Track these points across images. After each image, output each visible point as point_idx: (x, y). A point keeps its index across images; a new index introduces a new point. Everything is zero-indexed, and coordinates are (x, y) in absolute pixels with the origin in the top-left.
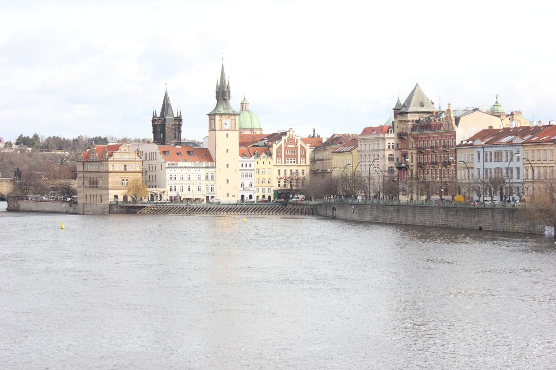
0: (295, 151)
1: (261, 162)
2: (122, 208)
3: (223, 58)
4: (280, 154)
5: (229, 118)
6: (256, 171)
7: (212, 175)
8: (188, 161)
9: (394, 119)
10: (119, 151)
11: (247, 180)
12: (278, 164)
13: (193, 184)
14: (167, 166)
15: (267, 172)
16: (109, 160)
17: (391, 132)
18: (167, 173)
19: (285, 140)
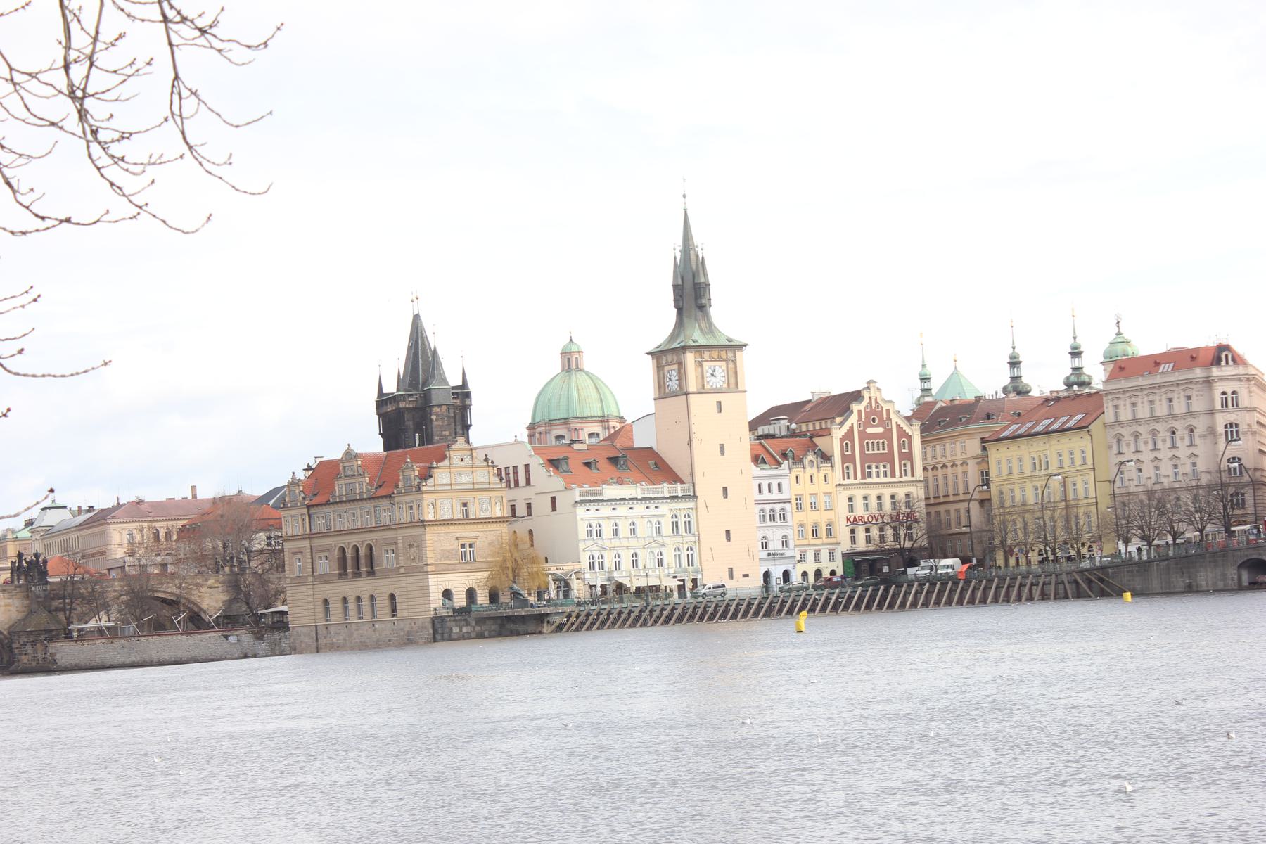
0: (886, 443)
1: (805, 478)
2: (485, 623)
3: (686, 193)
4: (849, 453)
5: (720, 359)
6: (794, 502)
7: (687, 519)
10: (446, 463)
11: (774, 529)
12: (847, 482)
13: (644, 547)
14: (578, 499)
15: (821, 505)
16: (424, 488)
17: (1227, 363)
18: (579, 518)
19: (860, 412)
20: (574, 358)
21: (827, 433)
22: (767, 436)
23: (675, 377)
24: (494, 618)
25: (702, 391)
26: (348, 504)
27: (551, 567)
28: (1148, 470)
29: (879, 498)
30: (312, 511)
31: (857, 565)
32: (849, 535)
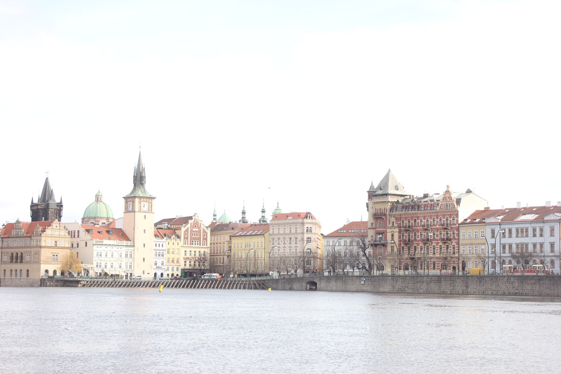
0: (199, 234)
1: (171, 243)
2: (58, 282)
5: (146, 201)
6: (167, 251)
8: (112, 240)
9: (369, 201)
10: (51, 227)
11: (160, 259)
12: (185, 246)
13: (115, 261)
14: (95, 243)
15: (176, 253)
16: (42, 235)
17: (309, 218)
18: (94, 250)
19: (191, 223)
20: (99, 198)
21: (180, 229)
22: (160, 228)
23: (131, 206)
24: (62, 281)
25: (140, 211)
26: (16, 238)
27: (83, 265)
28: (282, 250)
29: (195, 252)
30: (3, 239)
31: (186, 273)
32: (184, 263)
